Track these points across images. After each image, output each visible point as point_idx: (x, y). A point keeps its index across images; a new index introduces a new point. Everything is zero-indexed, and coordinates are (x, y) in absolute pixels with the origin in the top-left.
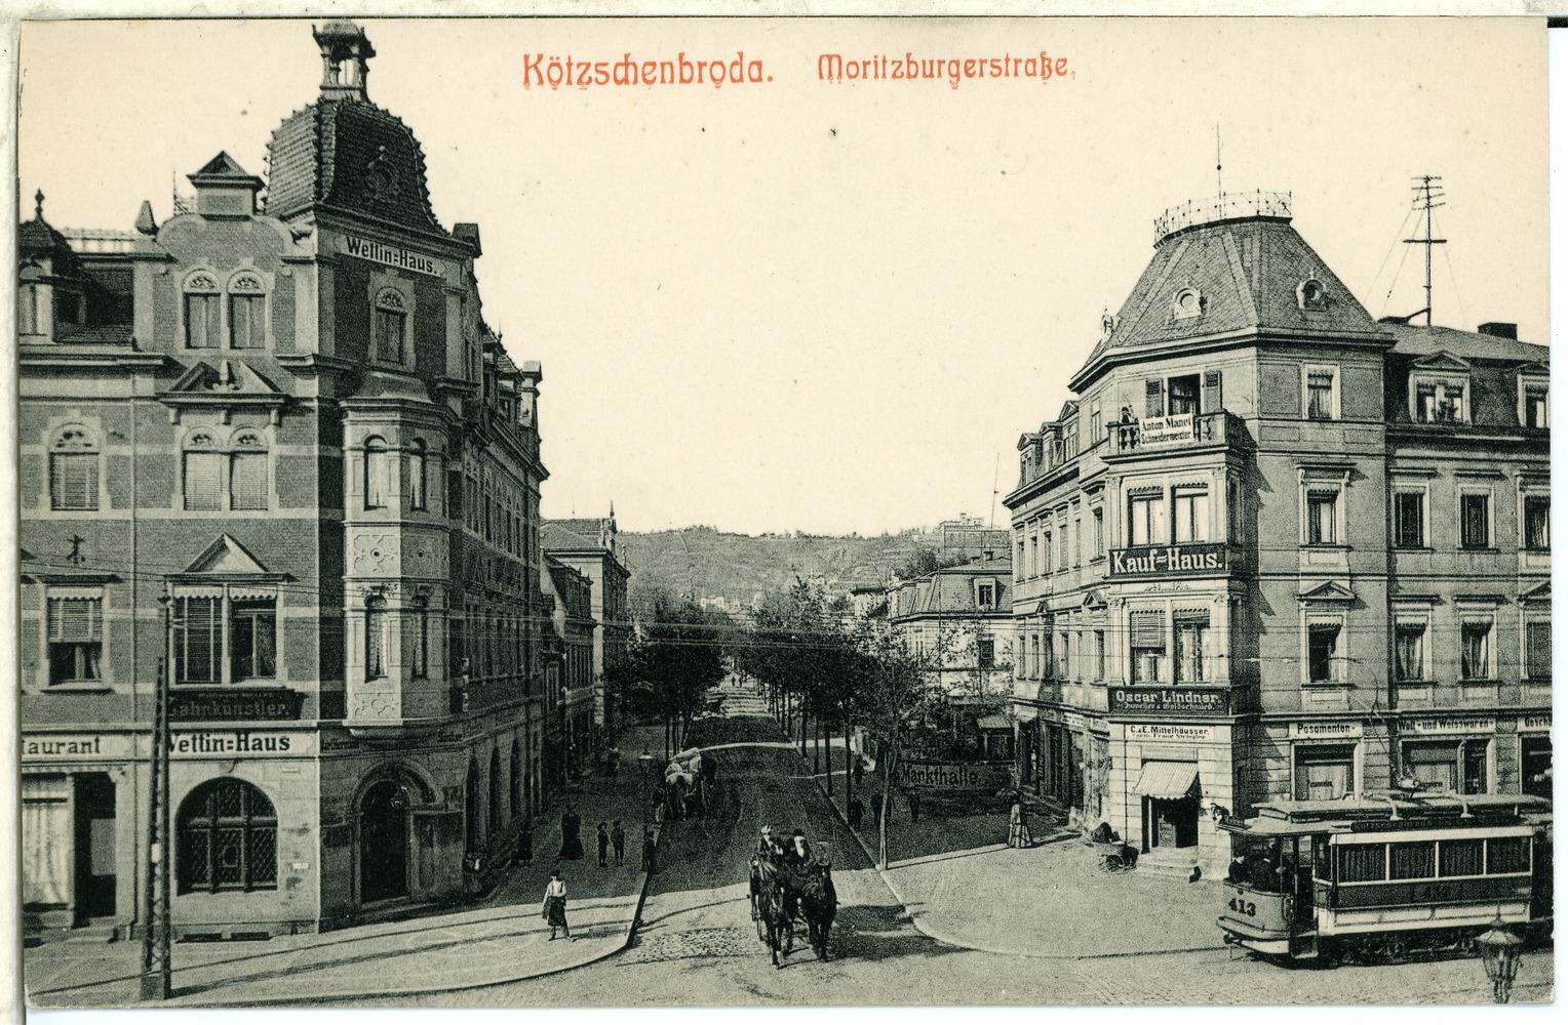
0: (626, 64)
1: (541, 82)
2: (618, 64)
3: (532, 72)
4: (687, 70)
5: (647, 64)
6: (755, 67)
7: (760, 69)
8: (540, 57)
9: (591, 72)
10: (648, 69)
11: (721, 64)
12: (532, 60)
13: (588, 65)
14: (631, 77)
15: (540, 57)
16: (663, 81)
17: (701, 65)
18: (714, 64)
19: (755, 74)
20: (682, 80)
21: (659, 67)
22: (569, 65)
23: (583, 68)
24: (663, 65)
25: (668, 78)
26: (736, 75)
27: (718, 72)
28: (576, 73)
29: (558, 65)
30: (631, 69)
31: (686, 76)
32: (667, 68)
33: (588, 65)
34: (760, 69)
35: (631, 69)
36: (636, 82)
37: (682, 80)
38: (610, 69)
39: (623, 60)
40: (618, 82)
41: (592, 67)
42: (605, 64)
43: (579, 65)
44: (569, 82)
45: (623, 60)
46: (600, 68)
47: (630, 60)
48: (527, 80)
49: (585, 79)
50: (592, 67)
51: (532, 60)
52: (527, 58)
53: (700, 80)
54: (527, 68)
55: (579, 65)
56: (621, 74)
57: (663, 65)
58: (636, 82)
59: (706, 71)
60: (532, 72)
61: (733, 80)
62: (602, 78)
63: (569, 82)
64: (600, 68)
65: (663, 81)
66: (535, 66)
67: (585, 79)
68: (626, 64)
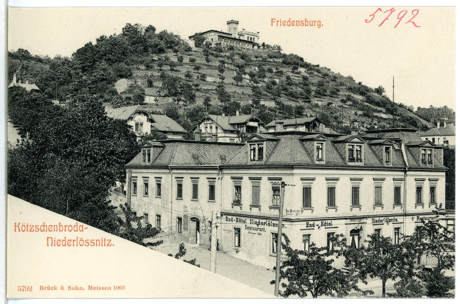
0: (44, 226)
1: (19, 231)
2: (41, 226)
5: (50, 226)
8: (19, 224)
9: (34, 228)
10: (50, 227)
11: (71, 226)
12: (17, 224)
14: (45, 230)
15: (19, 224)
16: (54, 231)
17: (65, 226)
20: (60, 231)
21: (53, 227)
22: (27, 226)
23: (31, 227)
33: (33, 226)
36: (46, 231)
37: (60, 231)
38: (39, 227)
40: (41, 231)
42: (38, 226)
44: (27, 231)
45: (43, 225)
46: (37, 227)
47: (45, 224)
48: (15, 231)
49: (32, 230)
51: (17, 224)
54: (15, 227)
56: (42, 228)
57: (54, 226)
58: (46, 231)
59: (67, 228)
62: (37, 230)
63: (27, 231)
65: (54, 231)
66: (18, 226)
67: (32, 230)
68: (44, 226)
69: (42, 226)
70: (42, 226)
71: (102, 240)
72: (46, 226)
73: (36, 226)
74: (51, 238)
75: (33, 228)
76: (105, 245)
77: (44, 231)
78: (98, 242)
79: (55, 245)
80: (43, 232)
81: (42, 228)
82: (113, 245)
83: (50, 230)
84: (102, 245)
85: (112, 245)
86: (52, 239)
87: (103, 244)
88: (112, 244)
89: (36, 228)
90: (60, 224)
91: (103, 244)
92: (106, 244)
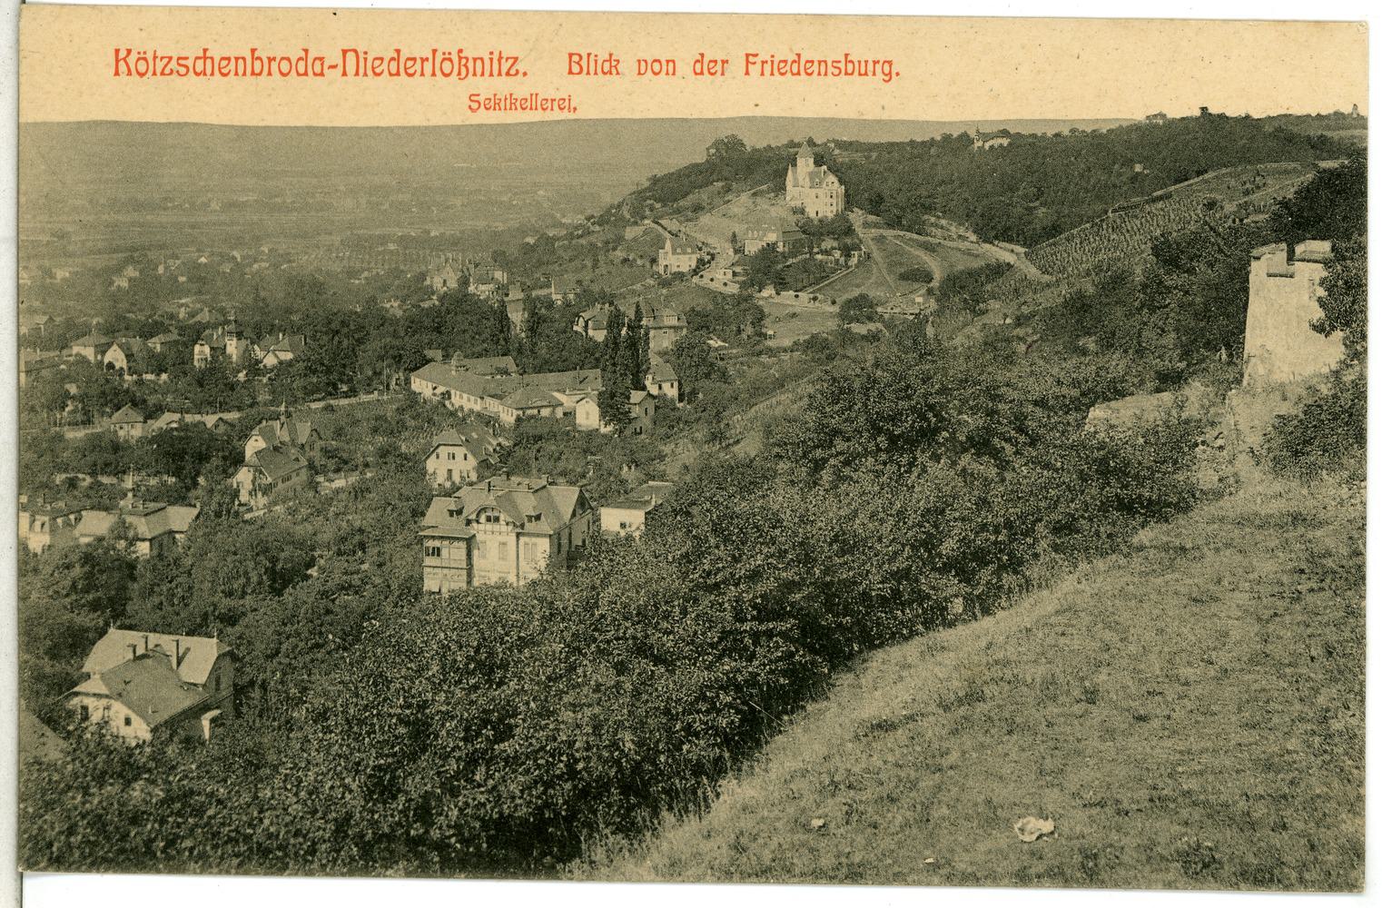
0: (205, 58)
1: (129, 73)
2: (197, 58)
3: (122, 63)
4: (258, 65)
6: (318, 63)
7: (322, 64)
8: (129, 52)
9: (173, 65)
10: (224, 63)
11: (288, 59)
12: (122, 54)
13: (170, 58)
14: (209, 71)
15: (129, 52)
16: (236, 74)
17: (270, 60)
18: (282, 59)
19: (318, 69)
20: (253, 73)
21: (233, 61)
22: (155, 58)
23: (166, 60)
24: (237, 59)
25: (241, 71)
26: (302, 70)
27: (285, 66)
28: (160, 65)
29: (145, 59)
30: (209, 62)
31: (257, 70)
32: (241, 62)
33: (170, 58)
34: (322, 64)
35: (209, 62)
36: (212, 74)
37: (253, 73)
38: (190, 63)
39: (201, 54)
40: (197, 74)
41: (174, 61)
42: (186, 58)
43: (162, 58)
44: (154, 74)
45: (201, 54)
46: (182, 62)
47: (208, 54)
48: (117, 73)
49: (167, 71)
50: (174, 61)
51: (122, 54)
52: (117, 51)
53: (270, 74)
54: (117, 61)
55: (162, 58)
56: (199, 68)
57: (237, 59)
58: (212, 74)
59: (274, 65)
60: (122, 63)
61: (298, 74)
62: (183, 70)
63: (154, 74)
64: (182, 62)
65: (236, 74)
66: (124, 59)
67: (167, 71)
68: (205, 58)
69: (200, 58)
70: (200, 58)
71: (491, 60)
72: (212, 59)
73: (179, 59)
74: (355, 51)
75: (170, 66)
76: (500, 74)
77: (205, 74)
78: (479, 63)
79: (365, 74)
80: (202, 76)
81: (199, 68)
82: (525, 74)
83: (224, 71)
84: (491, 75)
85: (520, 75)
86: (358, 57)
87: (495, 72)
88: (521, 71)
89: (179, 65)
90: (256, 56)
91: (495, 72)
92: (504, 71)
